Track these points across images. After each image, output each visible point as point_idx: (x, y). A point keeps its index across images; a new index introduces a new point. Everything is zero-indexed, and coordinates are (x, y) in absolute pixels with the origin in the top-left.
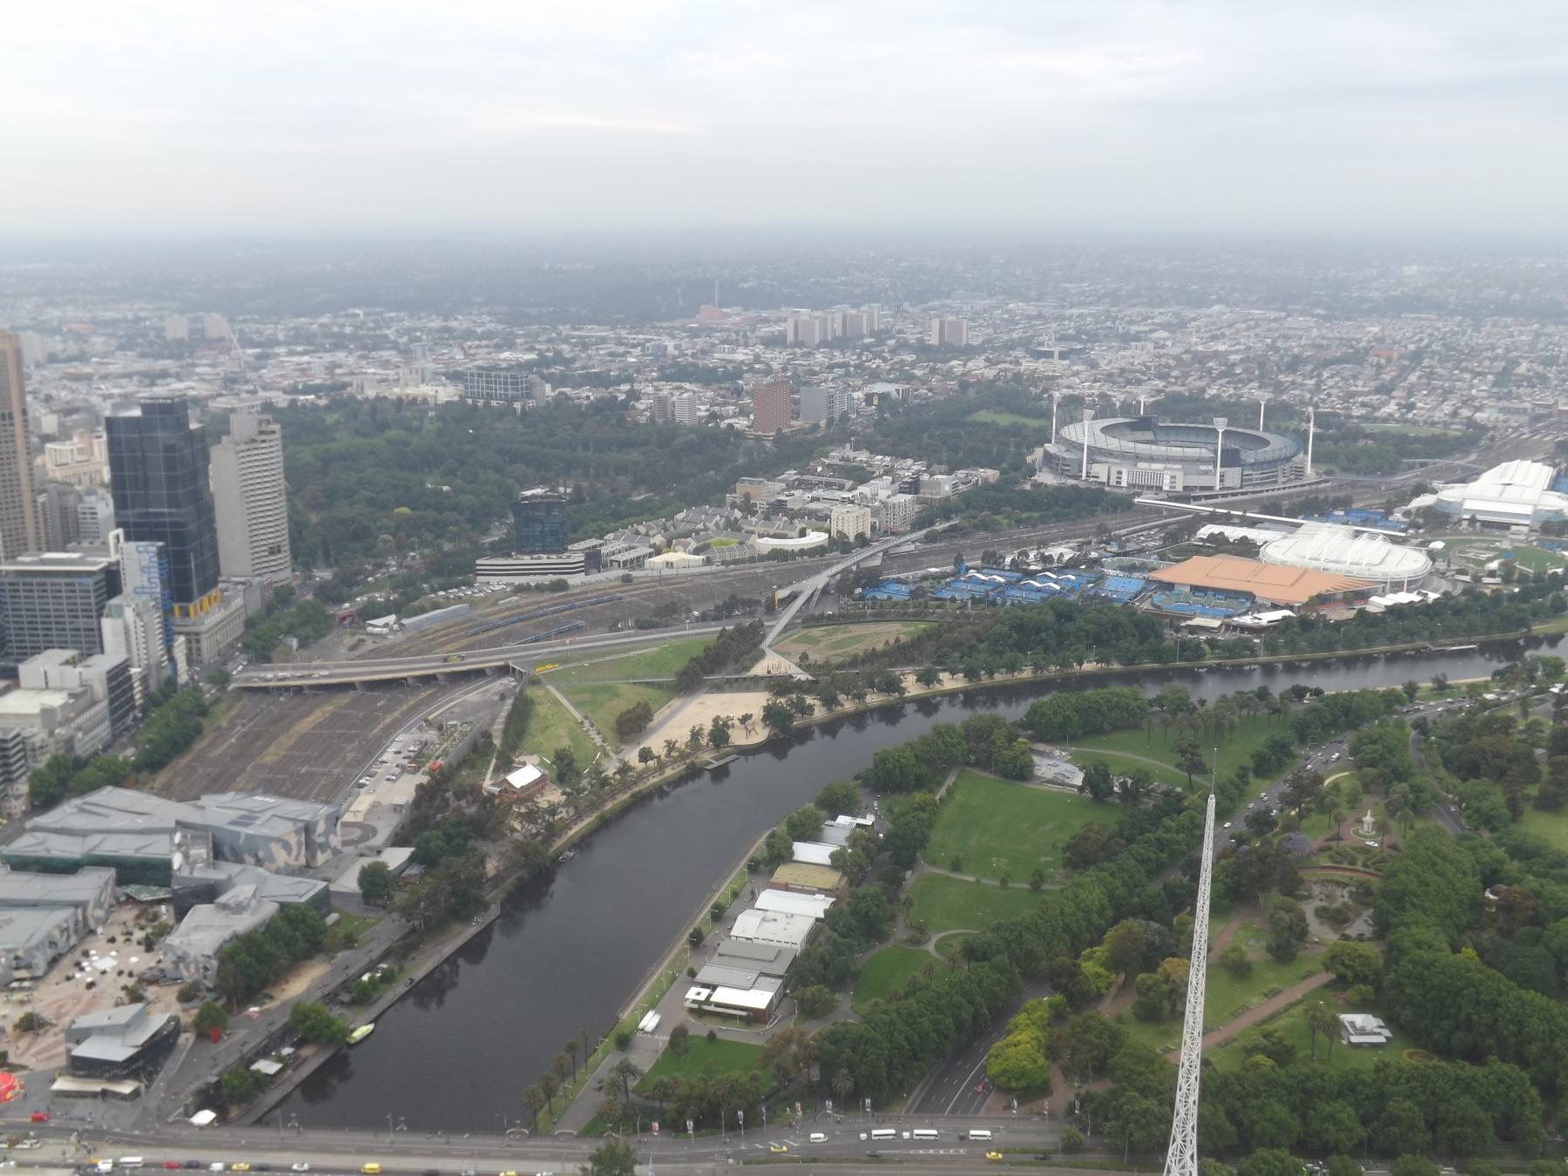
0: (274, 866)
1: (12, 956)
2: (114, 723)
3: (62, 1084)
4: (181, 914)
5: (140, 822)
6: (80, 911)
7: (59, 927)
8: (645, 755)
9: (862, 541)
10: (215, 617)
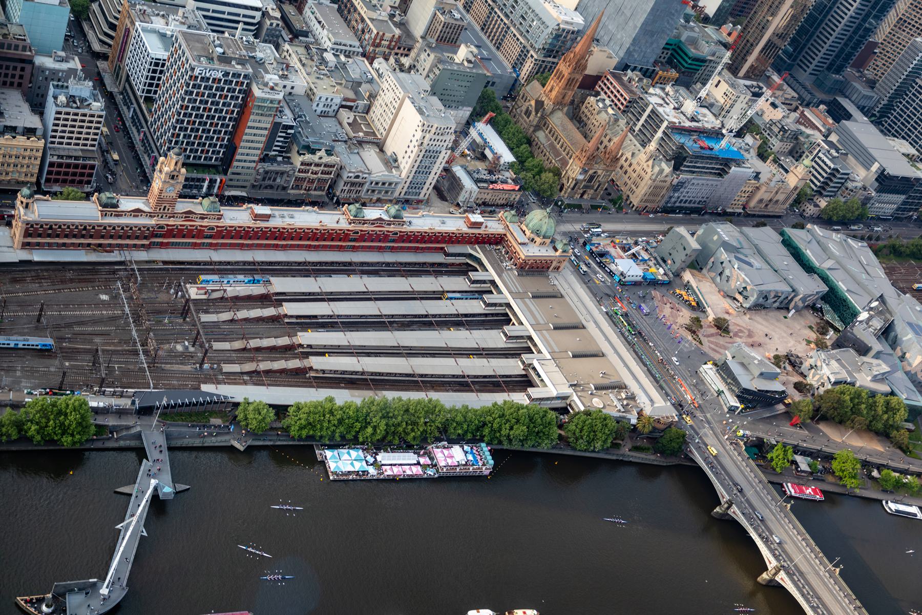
0: (908, 369)
1: (744, 285)
2: (898, 209)
4: (838, 345)
6: (793, 294)
7: (777, 292)
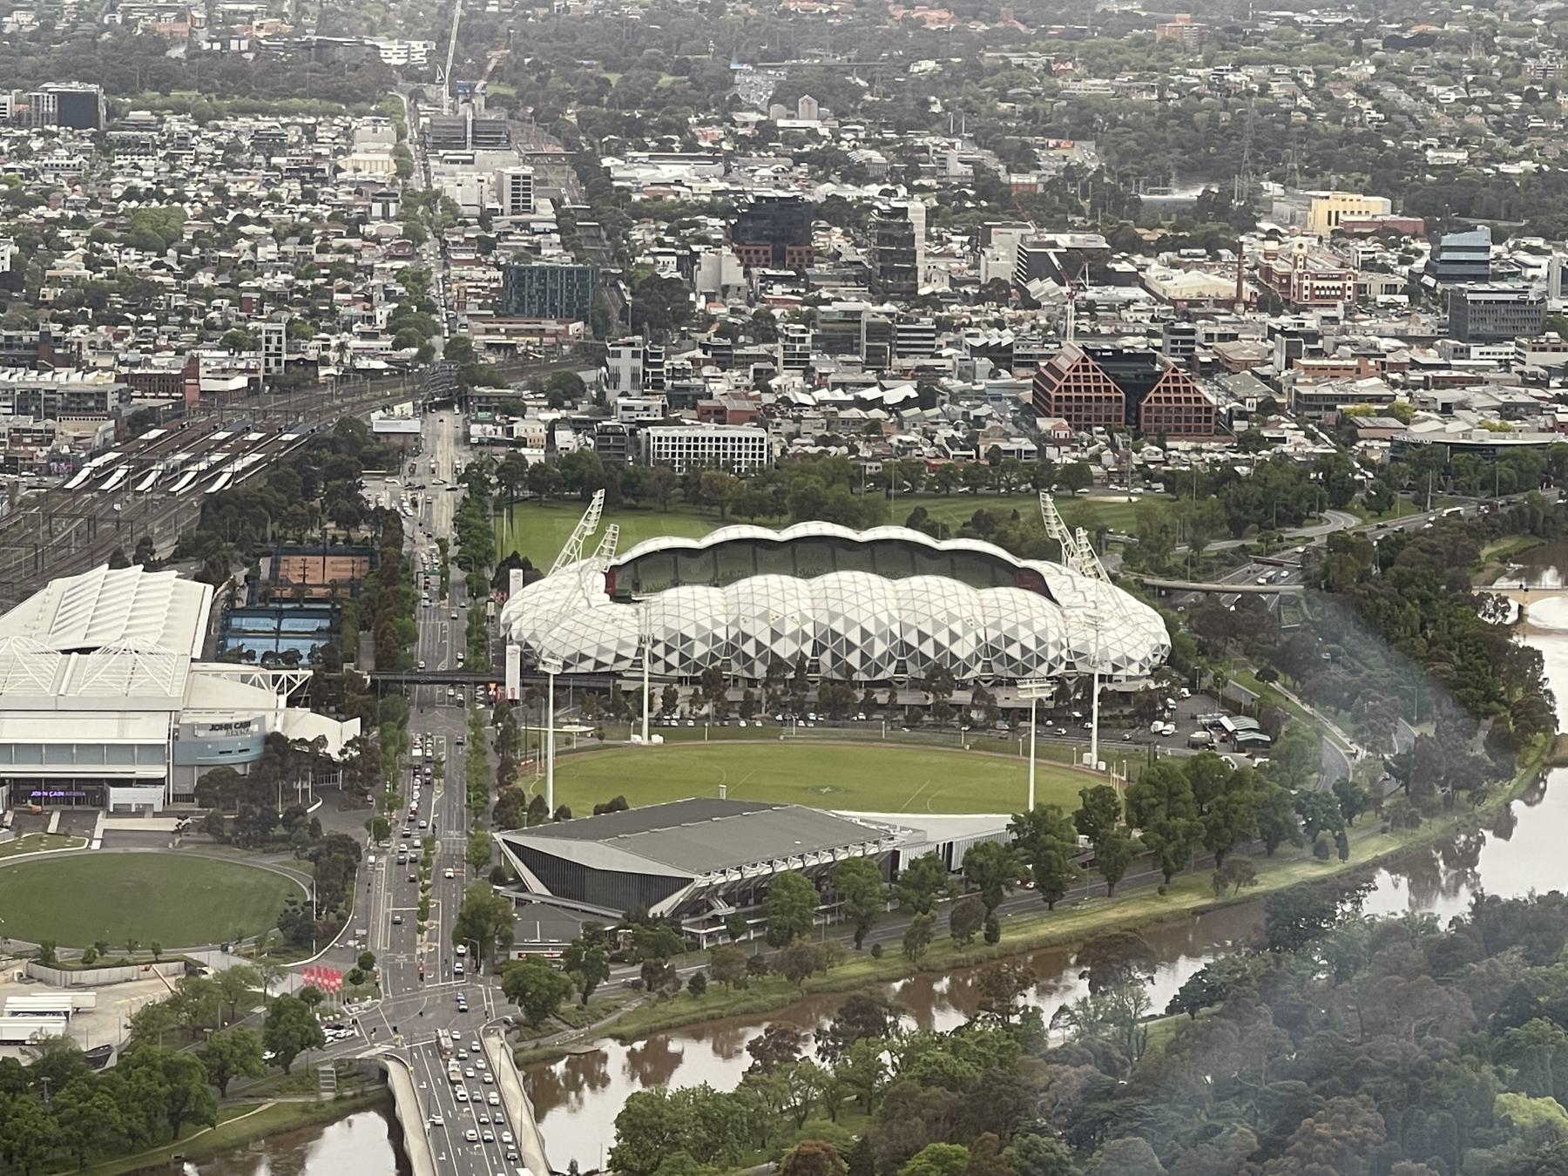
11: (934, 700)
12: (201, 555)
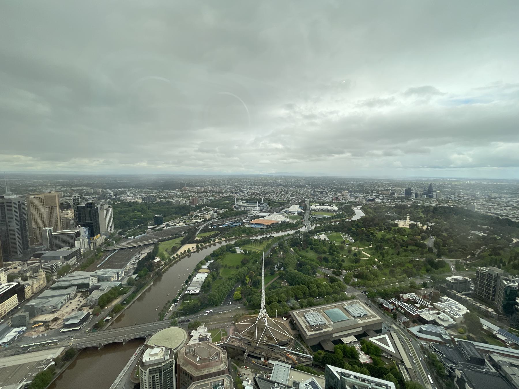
3: (62, 330)
4: (91, 293)
5: (83, 277)
8: (177, 255)
9: (209, 220)
10: (99, 239)
11: (328, 211)
12: (299, 204)
